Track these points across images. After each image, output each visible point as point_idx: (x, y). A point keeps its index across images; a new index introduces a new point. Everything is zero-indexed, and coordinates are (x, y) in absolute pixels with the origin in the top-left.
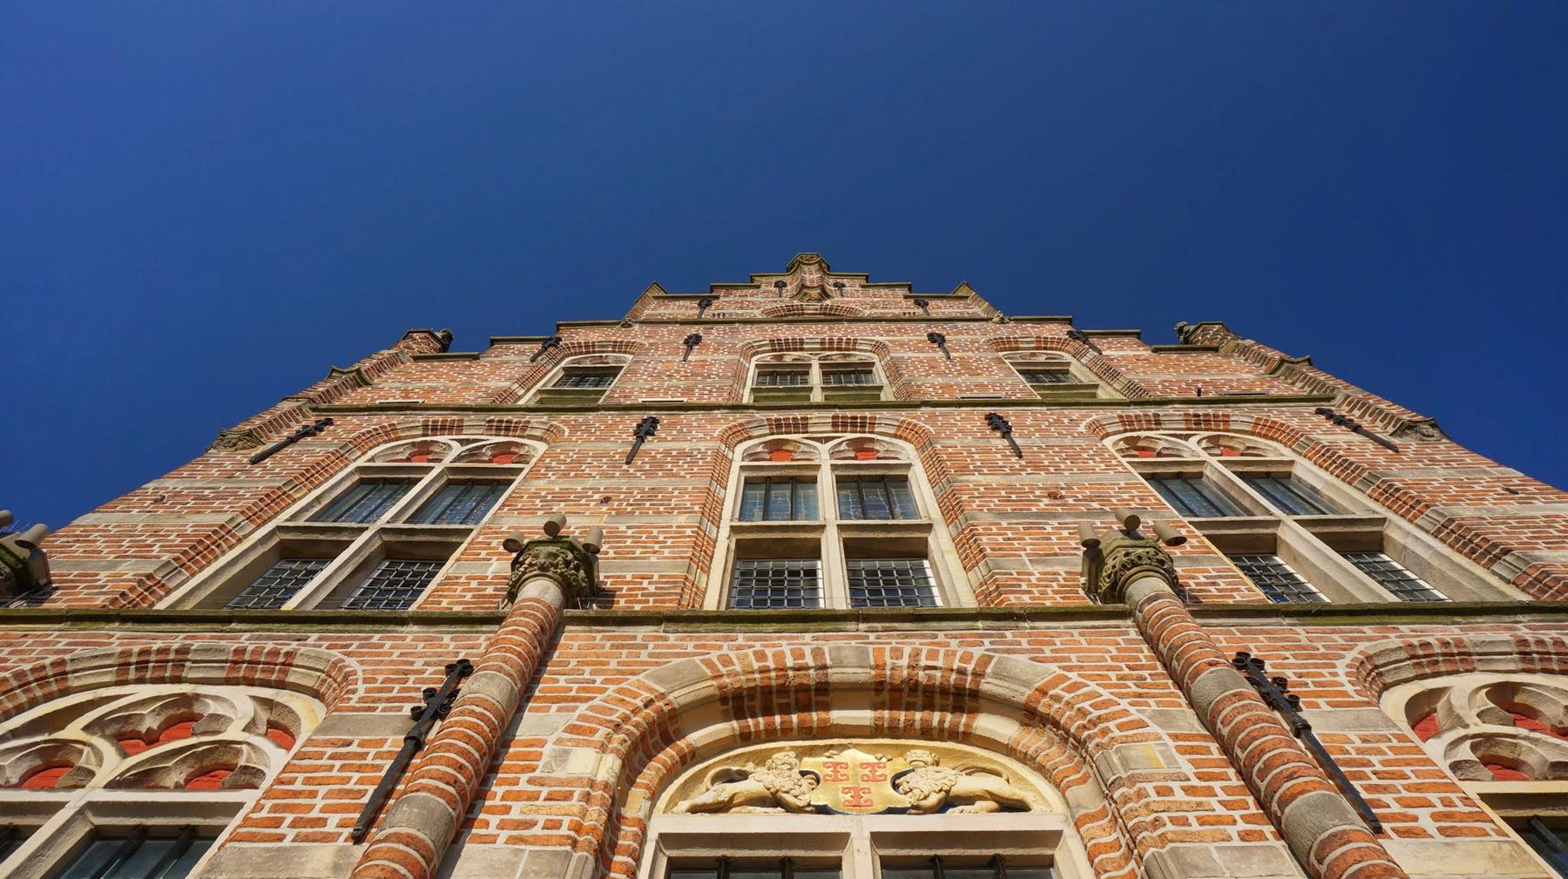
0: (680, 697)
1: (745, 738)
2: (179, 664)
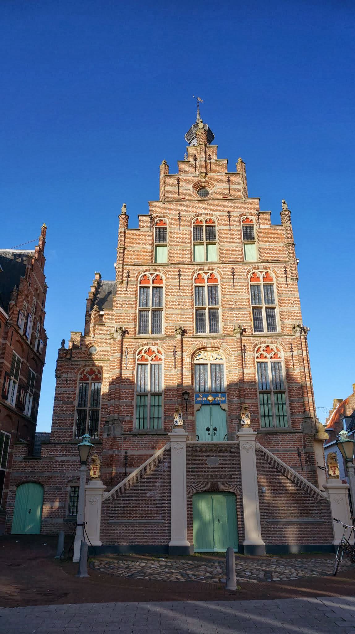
0: (194, 350)
1: (200, 351)
2: (147, 345)
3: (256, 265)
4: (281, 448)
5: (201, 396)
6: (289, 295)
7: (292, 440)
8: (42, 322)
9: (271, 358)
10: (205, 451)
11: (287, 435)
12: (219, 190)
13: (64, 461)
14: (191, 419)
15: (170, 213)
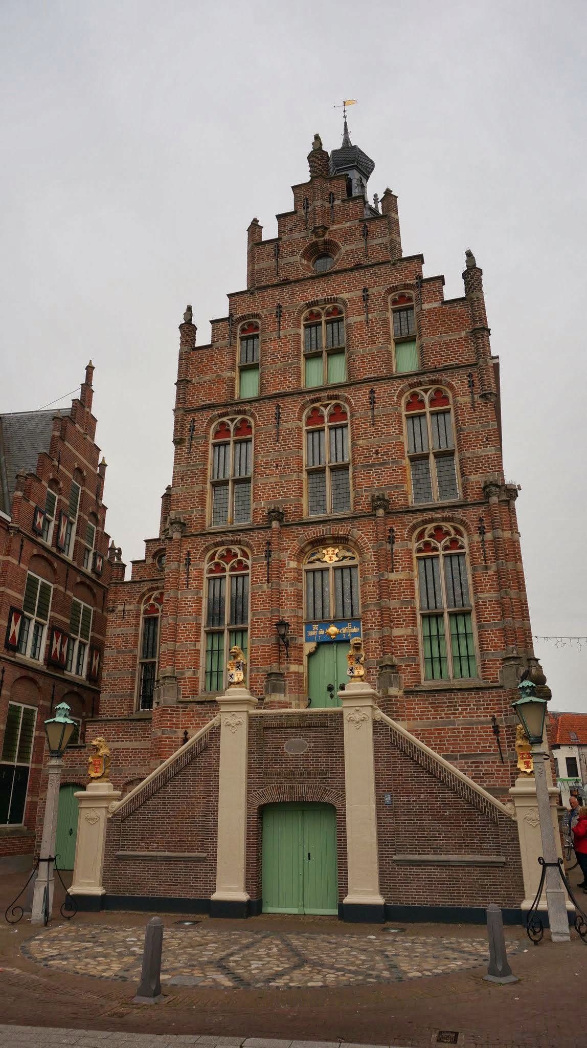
3: (415, 380)
4: (461, 718)
5: (315, 627)
6: (479, 425)
8: (100, 522)
9: (446, 548)
10: (282, 728)
11: (473, 693)
12: (348, 253)
13: (120, 749)
14: (297, 671)
15: (263, 307)
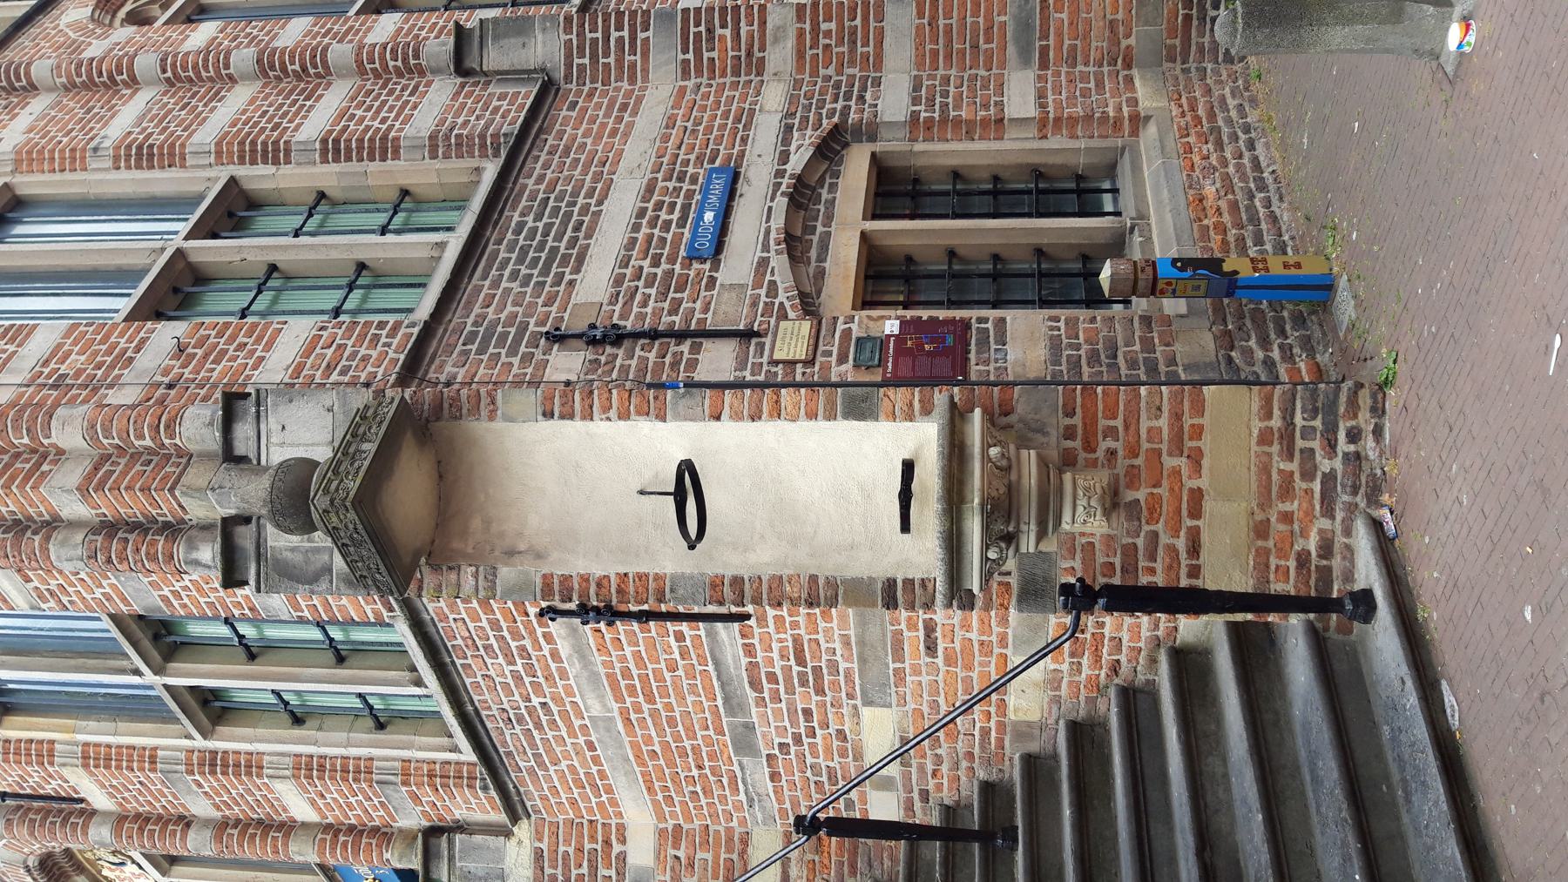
7: (493, 641)
